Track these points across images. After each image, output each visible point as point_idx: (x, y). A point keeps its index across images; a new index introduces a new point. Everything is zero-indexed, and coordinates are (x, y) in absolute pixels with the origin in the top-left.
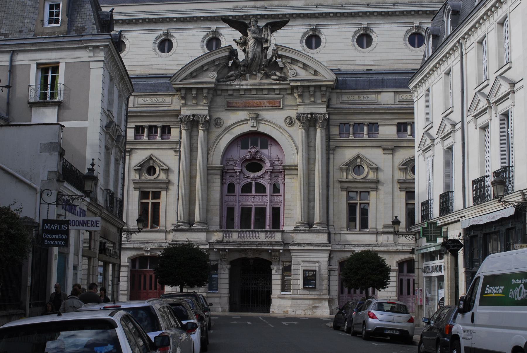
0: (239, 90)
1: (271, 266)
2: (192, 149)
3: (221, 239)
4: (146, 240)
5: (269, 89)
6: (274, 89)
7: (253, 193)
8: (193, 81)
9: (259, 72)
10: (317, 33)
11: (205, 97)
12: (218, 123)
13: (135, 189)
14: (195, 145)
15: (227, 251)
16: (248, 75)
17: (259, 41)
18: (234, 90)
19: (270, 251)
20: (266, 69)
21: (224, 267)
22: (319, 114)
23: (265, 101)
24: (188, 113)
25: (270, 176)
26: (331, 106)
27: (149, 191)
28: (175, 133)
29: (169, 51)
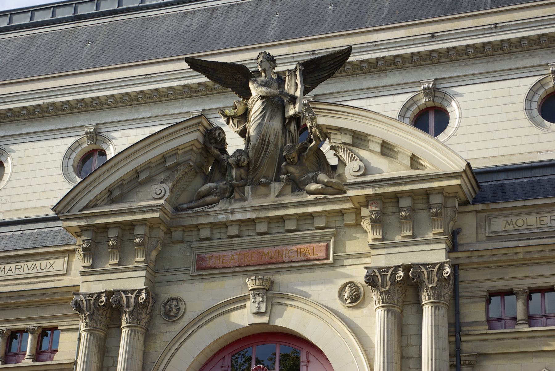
0: (225, 225)
6: (311, 216)
9: (278, 180)
12: (172, 311)
16: (248, 189)
17: (276, 103)
18: (213, 226)
22: (424, 265)
26: (460, 248)
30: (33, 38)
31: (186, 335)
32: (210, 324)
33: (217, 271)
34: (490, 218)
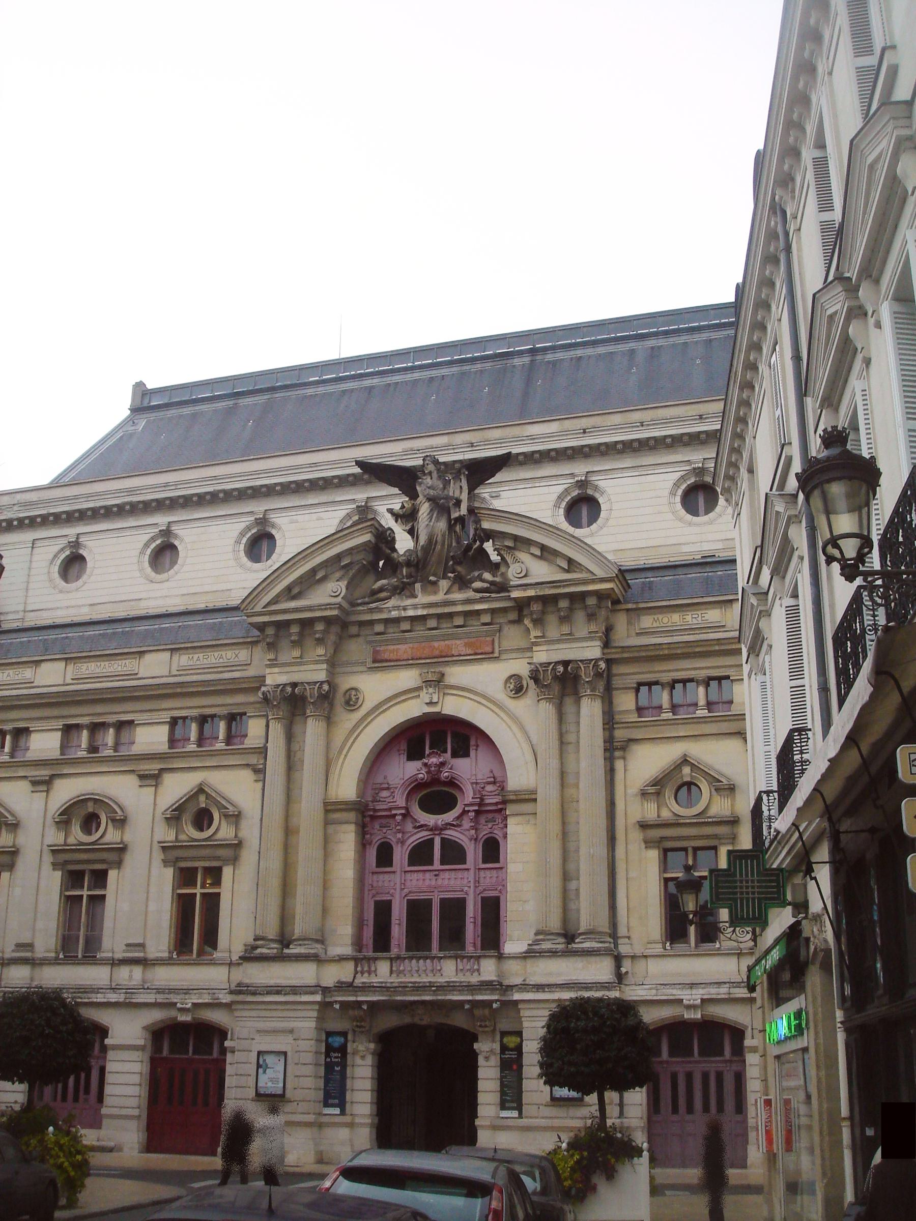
0: (397, 621)
1: (476, 1046)
2: (291, 765)
3: (349, 979)
4: (185, 984)
5: (467, 614)
6: (478, 613)
7: (437, 865)
8: (293, 604)
9: (445, 577)
10: (590, 492)
11: (320, 641)
12: (352, 701)
13: (166, 863)
14: (298, 755)
15: (365, 1007)
16: (418, 586)
18: (387, 621)
19: (467, 1007)
20: (459, 568)
21: (361, 1048)
22: (581, 661)
23: (458, 642)
24: (283, 679)
25: (476, 820)
27: (196, 868)
28: (255, 729)
29: (268, 558)
30: (194, 416)
32: (388, 712)
33: (392, 664)
34: (639, 616)
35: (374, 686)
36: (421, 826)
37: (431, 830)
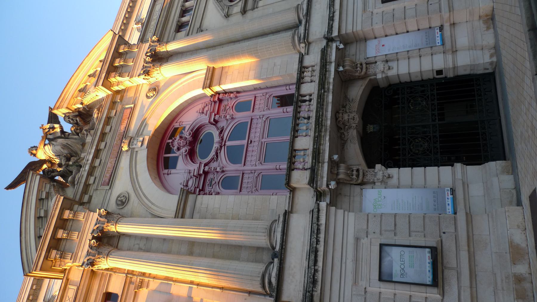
31: (139, 189)
35: (122, 184)
36: (217, 154)
37: (221, 147)
